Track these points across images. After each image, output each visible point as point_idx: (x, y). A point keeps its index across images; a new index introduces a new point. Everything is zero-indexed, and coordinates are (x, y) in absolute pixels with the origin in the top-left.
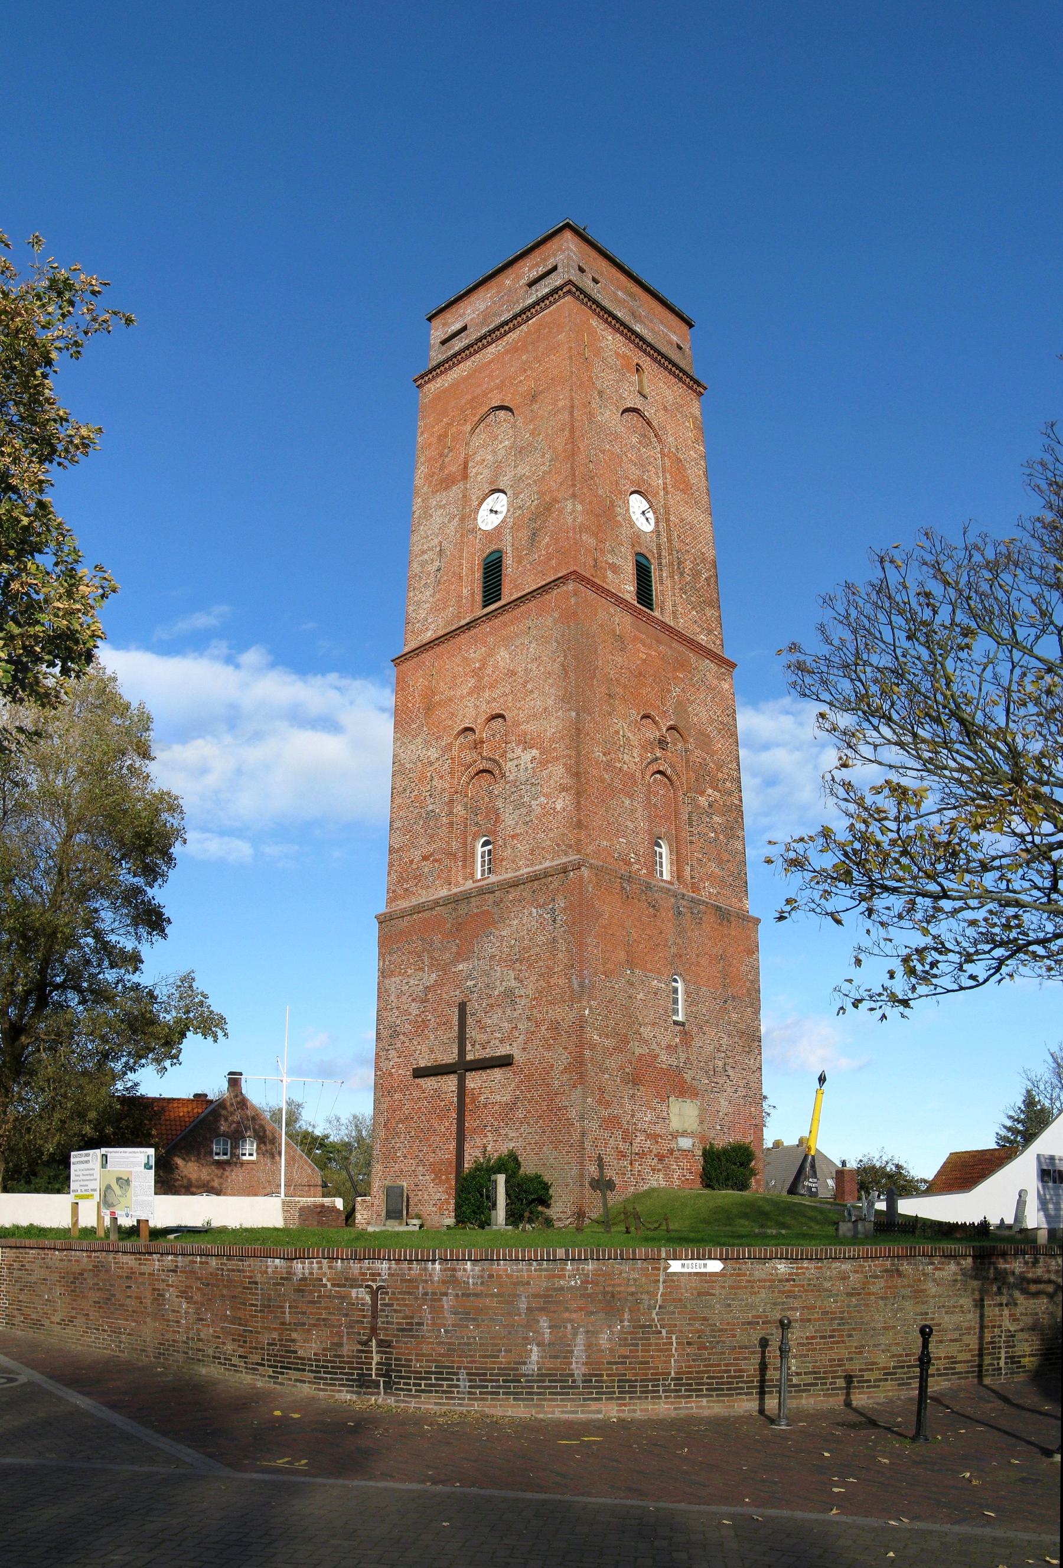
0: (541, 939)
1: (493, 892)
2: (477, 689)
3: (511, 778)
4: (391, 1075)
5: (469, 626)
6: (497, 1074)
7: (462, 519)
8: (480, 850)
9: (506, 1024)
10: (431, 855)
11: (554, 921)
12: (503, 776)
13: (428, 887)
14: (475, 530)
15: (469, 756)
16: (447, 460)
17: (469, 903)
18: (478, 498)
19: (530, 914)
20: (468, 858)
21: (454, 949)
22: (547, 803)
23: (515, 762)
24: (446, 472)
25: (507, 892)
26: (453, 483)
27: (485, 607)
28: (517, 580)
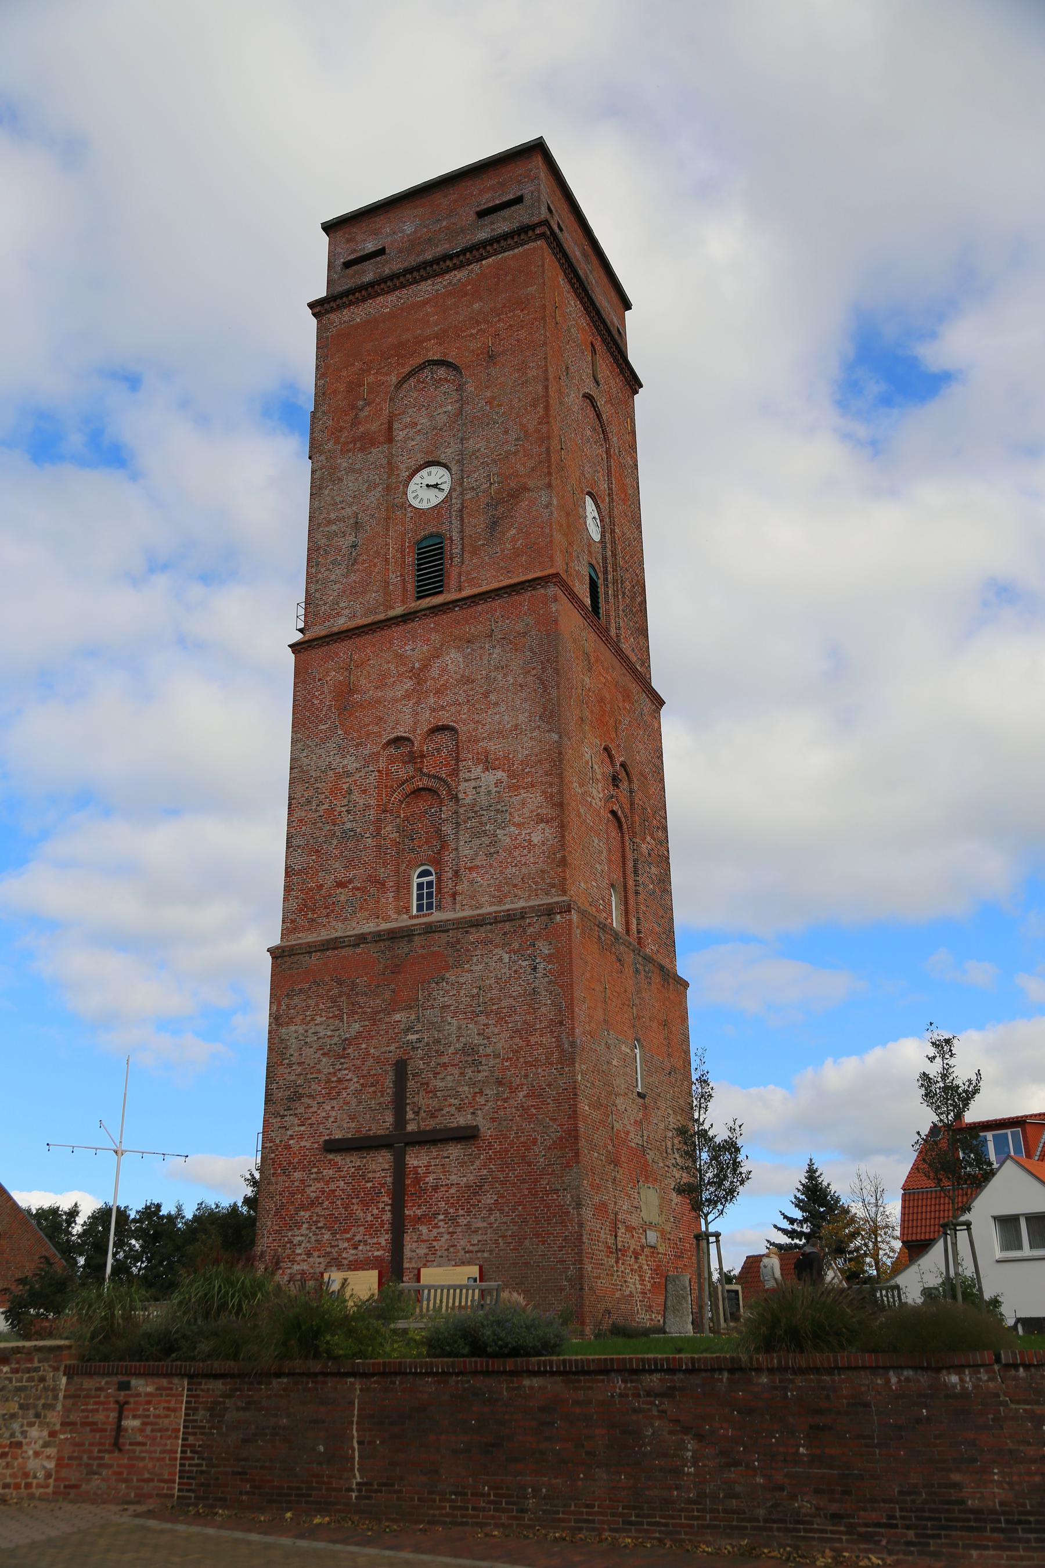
0: (516, 989)
1: (447, 931)
2: (418, 693)
3: (467, 801)
5: (406, 618)
6: (455, 1151)
7: (388, 489)
8: (416, 881)
9: (466, 1088)
10: (350, 881)
11: (535, 969)
12: (456, 798)
13: (346, 919)
14: (405, 505)
15: (403, 772)
16: (362, 414)
17: (410, 941)
18: (408, 468)
19: (501, 959)
20: (402, 887)
21: (388, 995)
22: (520, 834)
23: (473, 784)
24: (361, 429)
25: (467, 932)
26: (373, 444)
27: (419, 598)
28: (472, 573)
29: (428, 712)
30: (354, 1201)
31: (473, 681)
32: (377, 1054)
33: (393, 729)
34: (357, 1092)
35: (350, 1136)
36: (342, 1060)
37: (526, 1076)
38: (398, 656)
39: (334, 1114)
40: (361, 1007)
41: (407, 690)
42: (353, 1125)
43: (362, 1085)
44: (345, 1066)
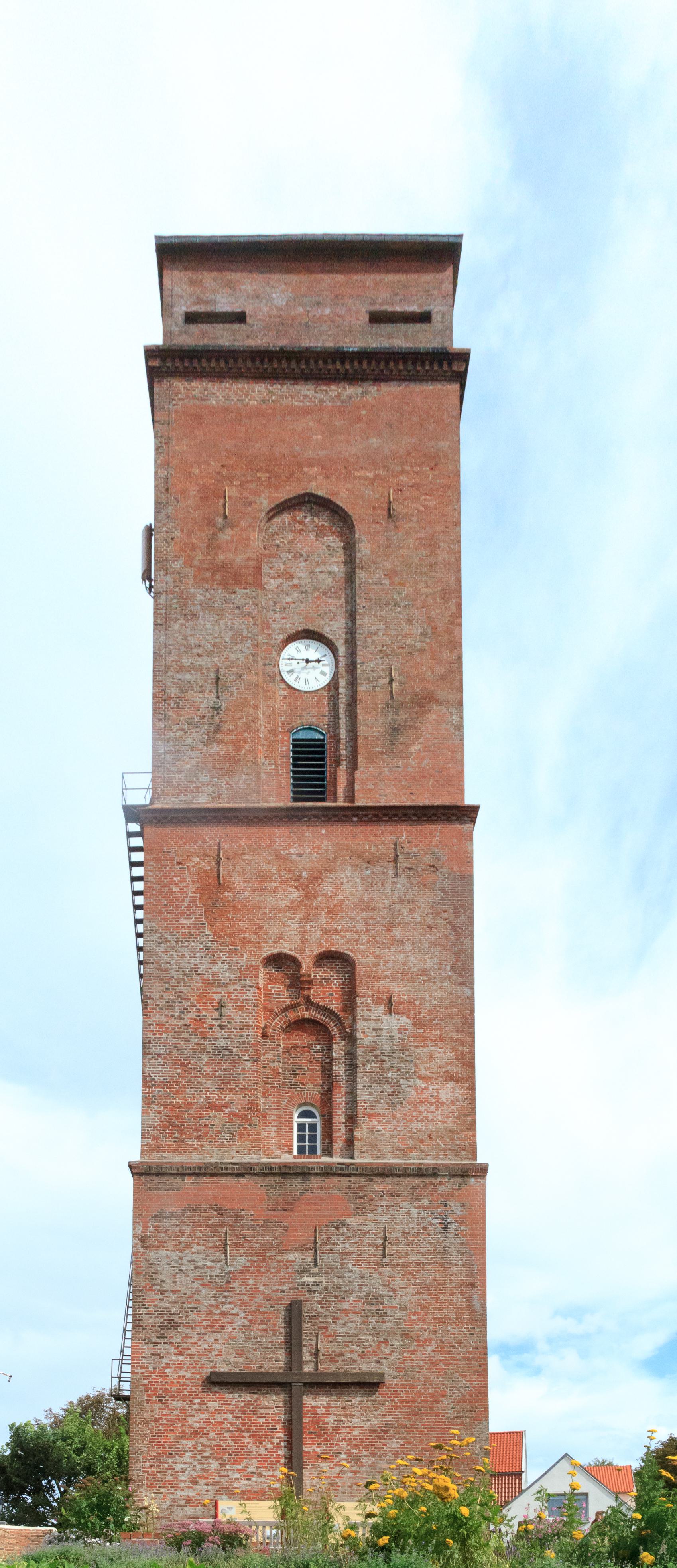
4: (164, 1375)
29: (319, 933)
30: (245, 1434)
31: (373, 909)
32: (267, 1291)
33: (275, 942)
34: (245, 1328)
35: (237, 1370)
36: (226, 1294)
37: (435, 1332)
38: (278, 857)
39: (218, 1347)
40: (246, 1241)
41: (292, 902)
42: (241, 1360)
43: (250, 1321)
44: (229, 1300)
